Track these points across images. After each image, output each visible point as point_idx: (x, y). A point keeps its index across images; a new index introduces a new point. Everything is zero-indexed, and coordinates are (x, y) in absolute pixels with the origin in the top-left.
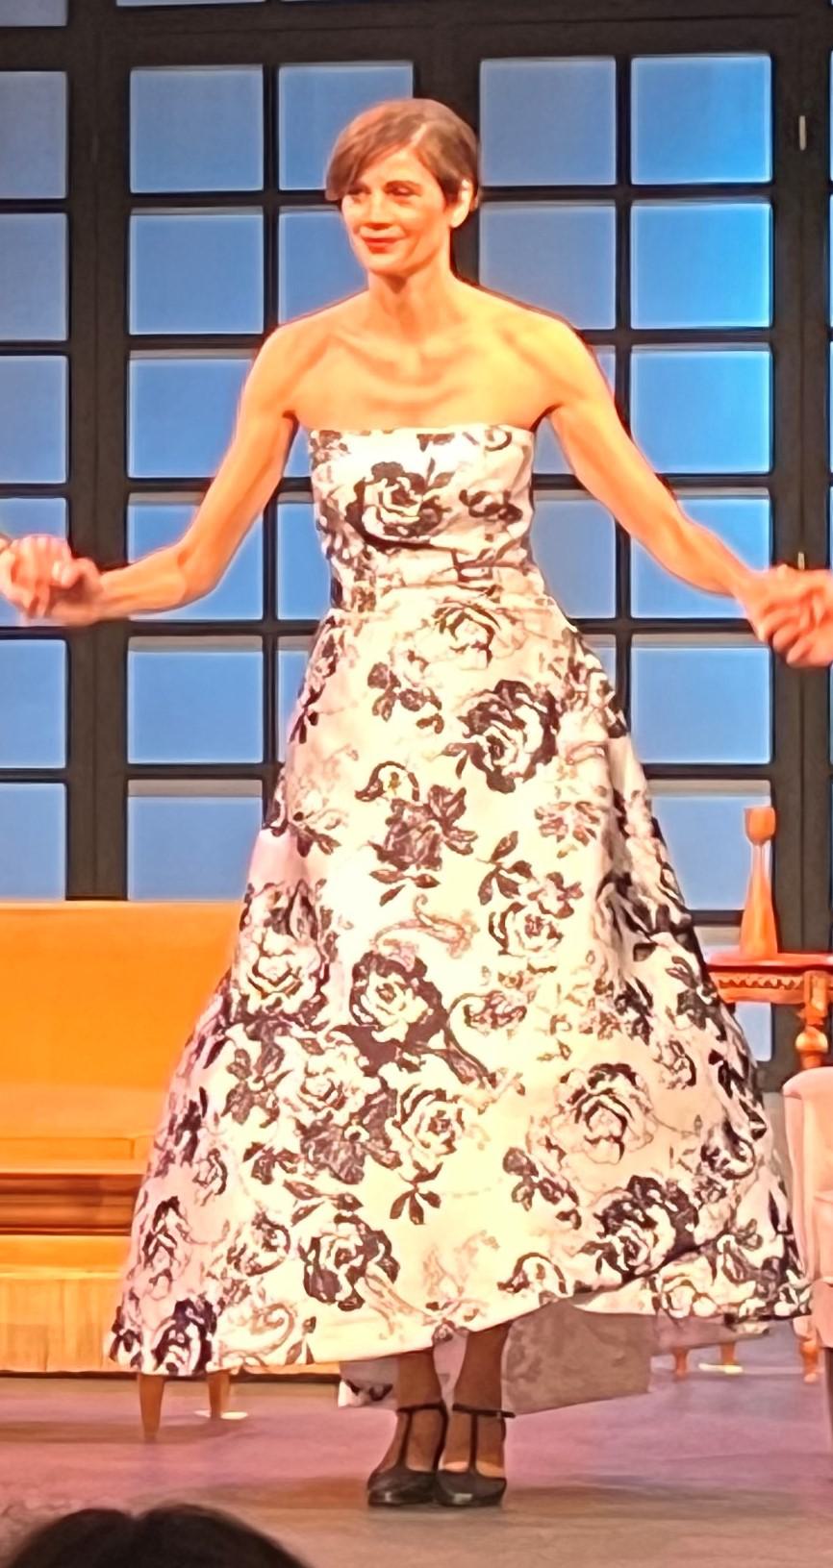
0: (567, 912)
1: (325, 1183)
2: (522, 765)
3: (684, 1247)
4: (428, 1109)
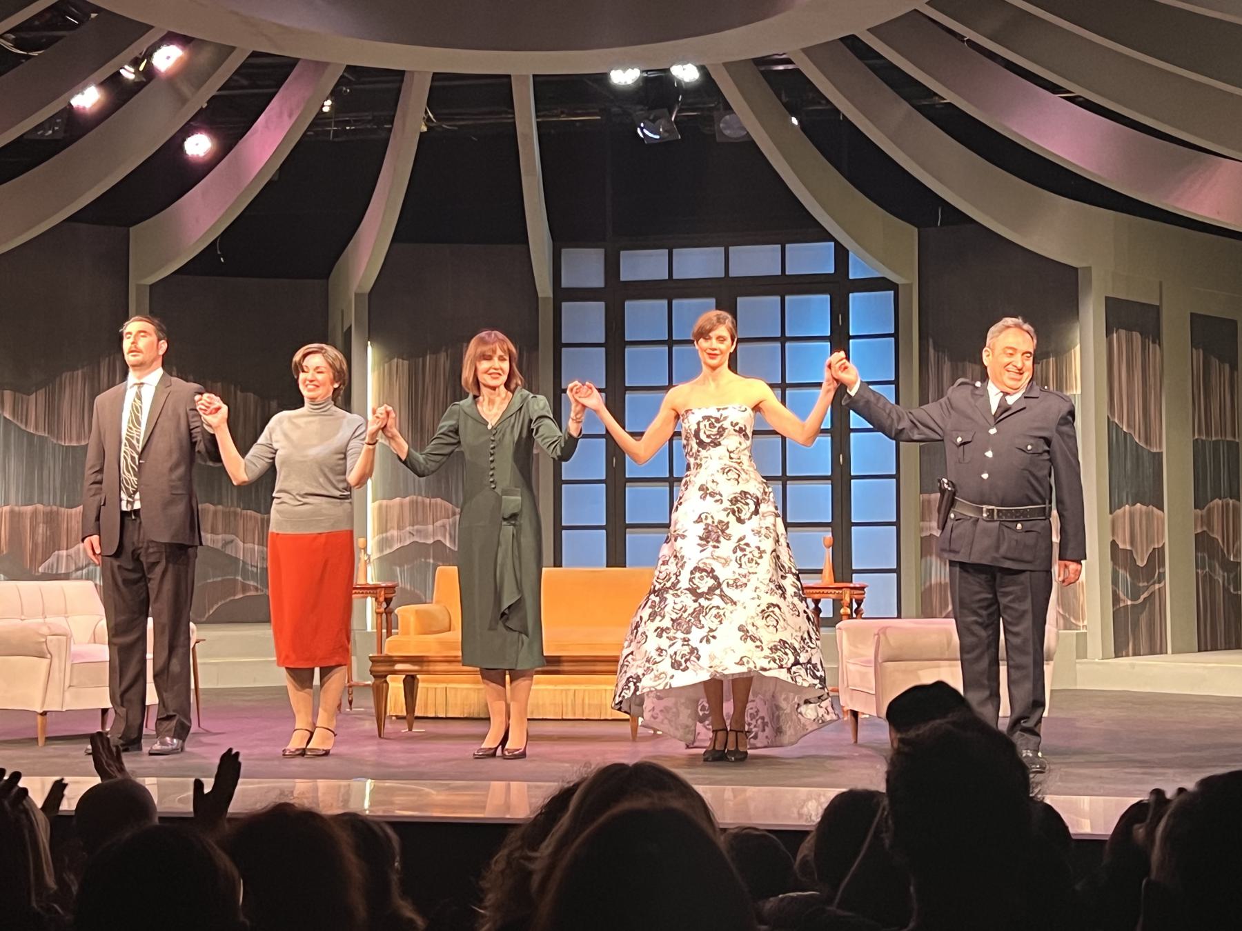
0: (761, 557)
1: (680, 635)
2: (748, 515)
3: (796, 663)
4: (714, 611)
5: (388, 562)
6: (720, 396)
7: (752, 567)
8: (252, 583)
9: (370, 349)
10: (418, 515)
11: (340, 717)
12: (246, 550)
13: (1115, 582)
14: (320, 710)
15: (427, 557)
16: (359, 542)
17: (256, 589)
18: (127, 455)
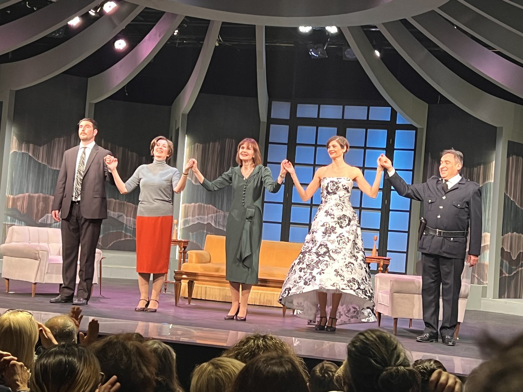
1: (309, 271)
2: (345, 225)
3: (359, 288)
4: (325, 262)
5: (187, 230)
6: (339, 173)
7: (345, 246)
8: (129, 234)
9: (186, 138)
10: (201, 211)
11: (161, 295)
12: (127, 220)
13: (501, 265)
15: (204, 229)
16: (175, 221)
17: (130, 237)
18: (78, 177)
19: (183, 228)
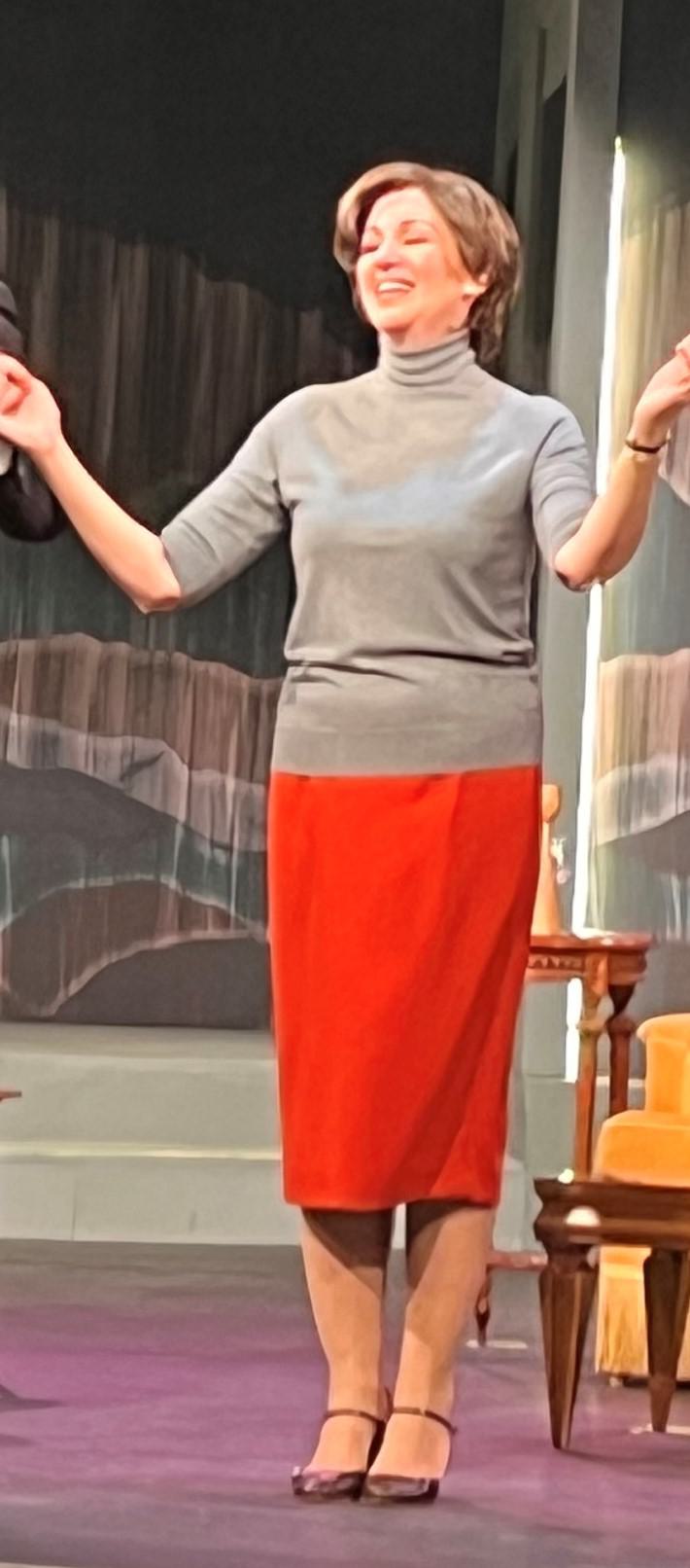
8: (211, 900)
9: (620, 159)
12: (198, 792)
14: (409, 1340)
17: (223, 919)
19: (615, 846)
